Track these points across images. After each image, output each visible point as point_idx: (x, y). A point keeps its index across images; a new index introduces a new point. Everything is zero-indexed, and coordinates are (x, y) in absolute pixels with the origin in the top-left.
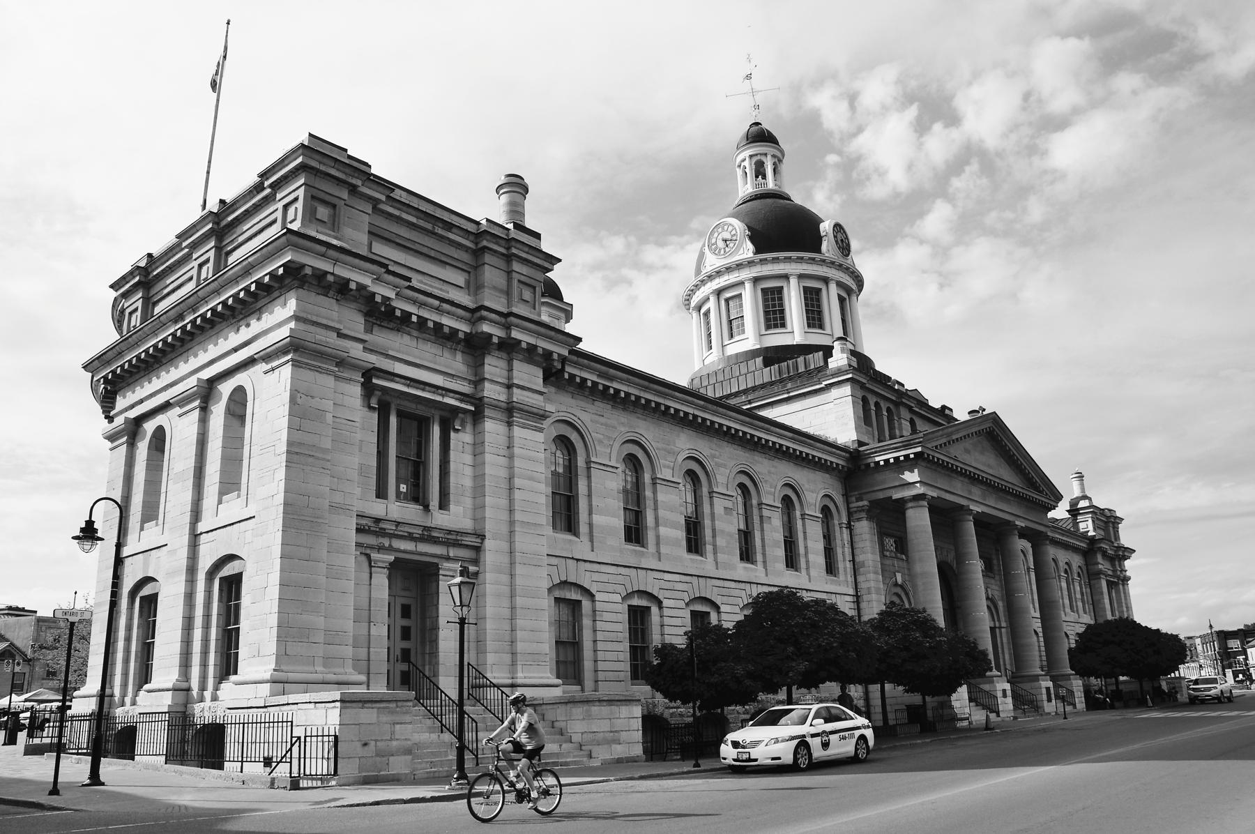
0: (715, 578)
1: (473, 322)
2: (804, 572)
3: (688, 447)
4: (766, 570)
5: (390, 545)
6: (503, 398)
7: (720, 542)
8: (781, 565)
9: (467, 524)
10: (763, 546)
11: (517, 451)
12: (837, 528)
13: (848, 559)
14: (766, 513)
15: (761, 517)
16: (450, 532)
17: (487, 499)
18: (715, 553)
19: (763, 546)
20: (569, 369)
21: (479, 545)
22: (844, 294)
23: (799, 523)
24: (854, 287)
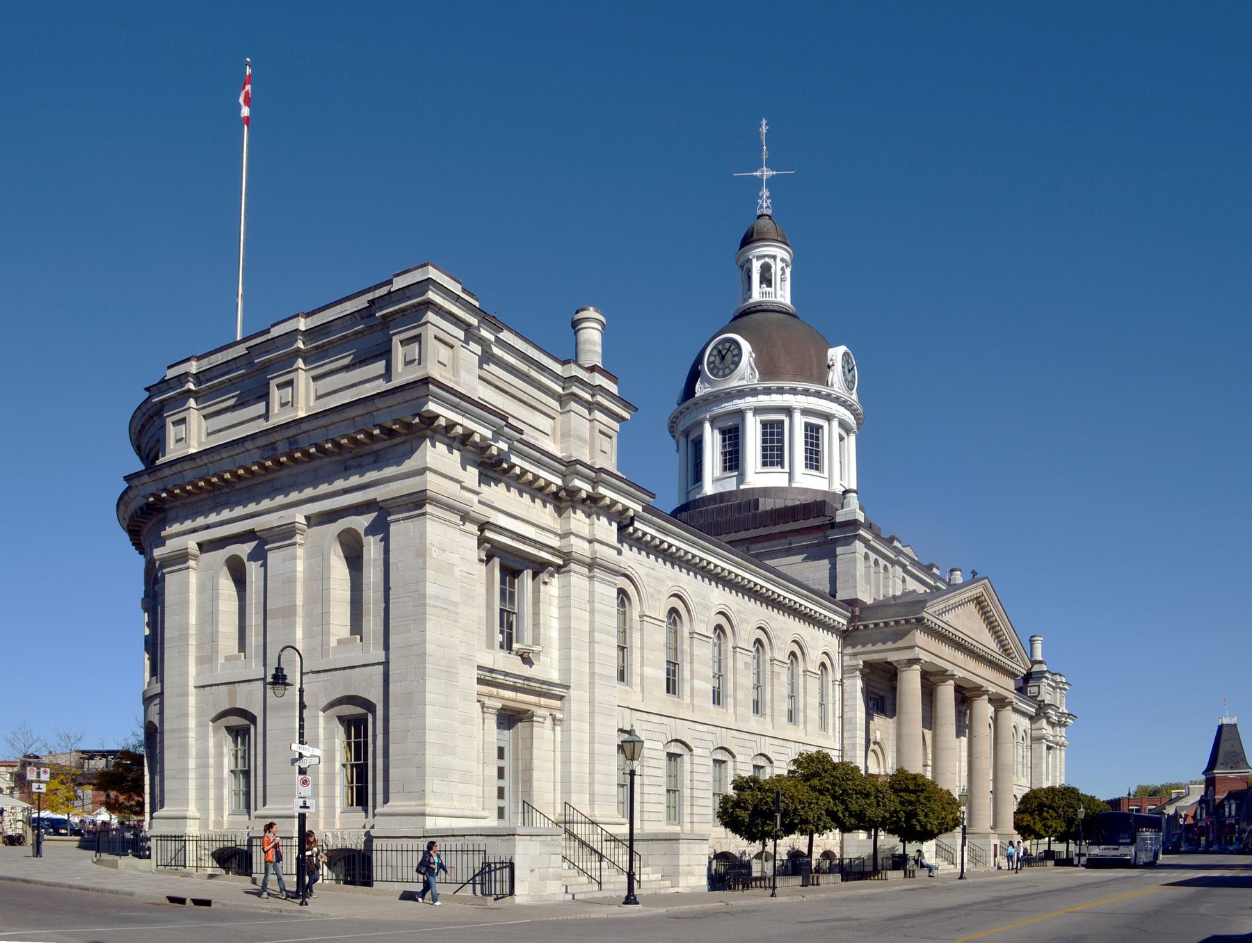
0: (734, 730)
1: (563, 476)
2: (802, 726)
3: (720, 602)
4: (773, 723)
5: (497, 693)
6: (588, 553)
7: (740, 695)
8: (785, 719)
9: (554, 676)
10: (772, 701)
11: (597, 606)
12: (830, 685)
13: (837, 715)
14: (777, 669)
15: (772, 672)
16: (544, 683)
17: (573, 651)
18: (735, 706)
19: (772, 701)
20: (637, 524)
23: (801, 679)
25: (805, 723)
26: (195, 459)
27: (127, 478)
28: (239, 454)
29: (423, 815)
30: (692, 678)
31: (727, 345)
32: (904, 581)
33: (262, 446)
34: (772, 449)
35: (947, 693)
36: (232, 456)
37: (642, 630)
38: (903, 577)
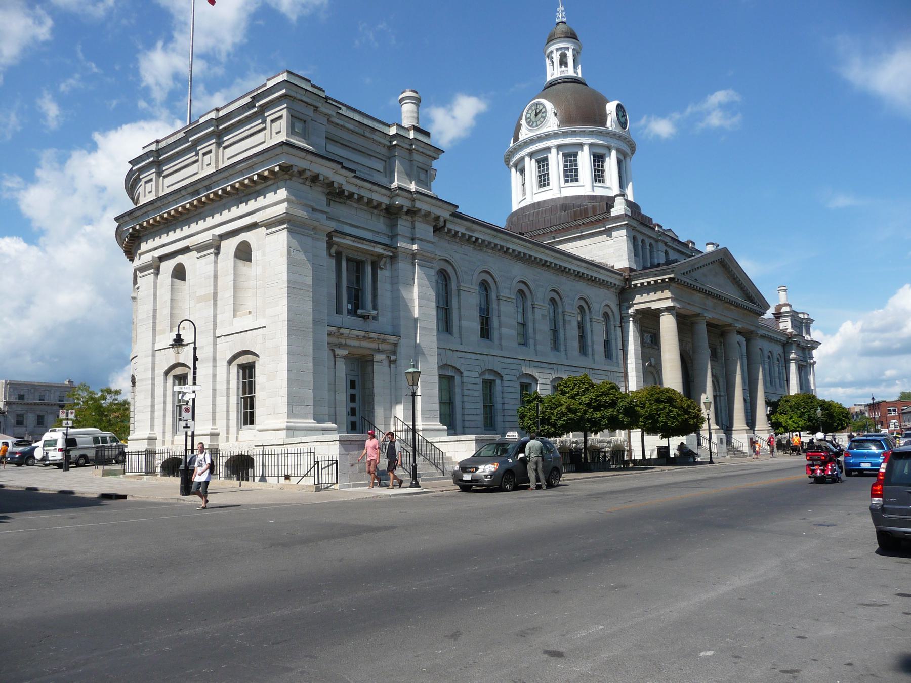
7: (539, 337)
8: (576, 352)
18: (535, 345)
21: (397, 342)
22: (621, 158)
24: (629, 152)
25: (593, 355)
26: (153, 203)
27: (117, 219)
28: (179, 198)
29: (288, 429)
30: (500, 326)
31: (534, 108)
32: (666, 253)
33: (192, 193)
34: (571, 171)
35: (702, 329)
36: (175, 200)
37: (459, 296)
38: (666, 250)
